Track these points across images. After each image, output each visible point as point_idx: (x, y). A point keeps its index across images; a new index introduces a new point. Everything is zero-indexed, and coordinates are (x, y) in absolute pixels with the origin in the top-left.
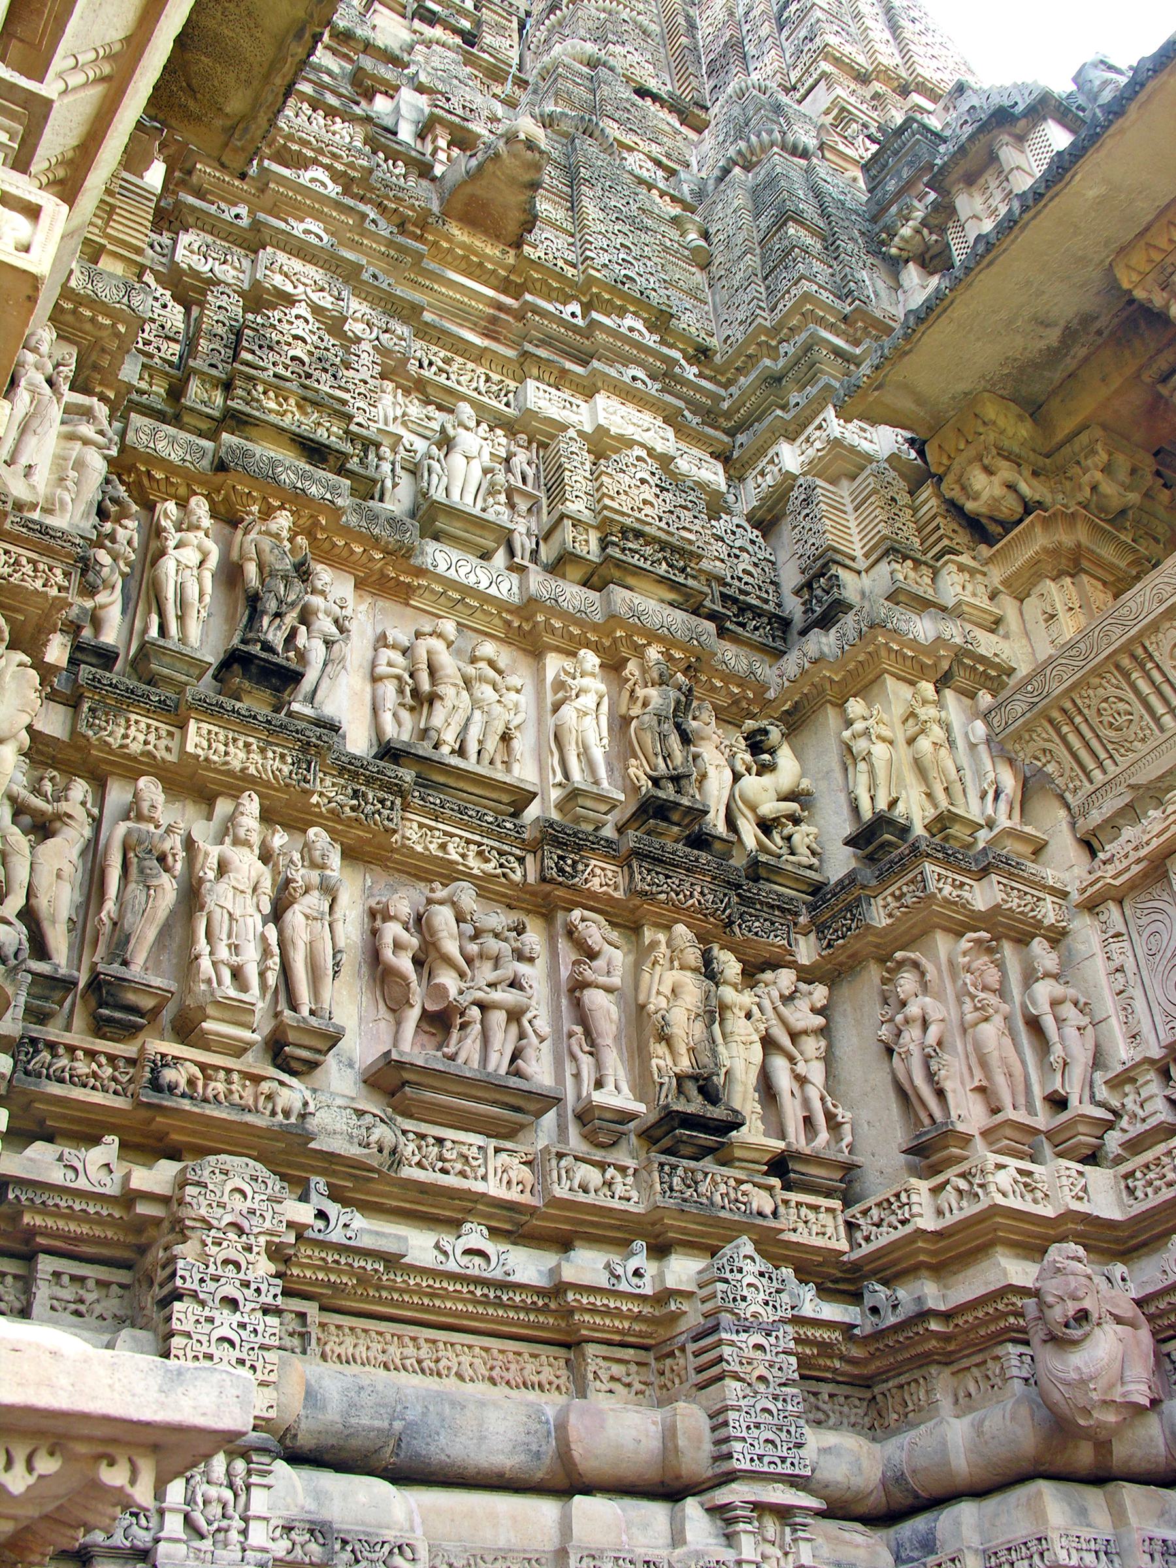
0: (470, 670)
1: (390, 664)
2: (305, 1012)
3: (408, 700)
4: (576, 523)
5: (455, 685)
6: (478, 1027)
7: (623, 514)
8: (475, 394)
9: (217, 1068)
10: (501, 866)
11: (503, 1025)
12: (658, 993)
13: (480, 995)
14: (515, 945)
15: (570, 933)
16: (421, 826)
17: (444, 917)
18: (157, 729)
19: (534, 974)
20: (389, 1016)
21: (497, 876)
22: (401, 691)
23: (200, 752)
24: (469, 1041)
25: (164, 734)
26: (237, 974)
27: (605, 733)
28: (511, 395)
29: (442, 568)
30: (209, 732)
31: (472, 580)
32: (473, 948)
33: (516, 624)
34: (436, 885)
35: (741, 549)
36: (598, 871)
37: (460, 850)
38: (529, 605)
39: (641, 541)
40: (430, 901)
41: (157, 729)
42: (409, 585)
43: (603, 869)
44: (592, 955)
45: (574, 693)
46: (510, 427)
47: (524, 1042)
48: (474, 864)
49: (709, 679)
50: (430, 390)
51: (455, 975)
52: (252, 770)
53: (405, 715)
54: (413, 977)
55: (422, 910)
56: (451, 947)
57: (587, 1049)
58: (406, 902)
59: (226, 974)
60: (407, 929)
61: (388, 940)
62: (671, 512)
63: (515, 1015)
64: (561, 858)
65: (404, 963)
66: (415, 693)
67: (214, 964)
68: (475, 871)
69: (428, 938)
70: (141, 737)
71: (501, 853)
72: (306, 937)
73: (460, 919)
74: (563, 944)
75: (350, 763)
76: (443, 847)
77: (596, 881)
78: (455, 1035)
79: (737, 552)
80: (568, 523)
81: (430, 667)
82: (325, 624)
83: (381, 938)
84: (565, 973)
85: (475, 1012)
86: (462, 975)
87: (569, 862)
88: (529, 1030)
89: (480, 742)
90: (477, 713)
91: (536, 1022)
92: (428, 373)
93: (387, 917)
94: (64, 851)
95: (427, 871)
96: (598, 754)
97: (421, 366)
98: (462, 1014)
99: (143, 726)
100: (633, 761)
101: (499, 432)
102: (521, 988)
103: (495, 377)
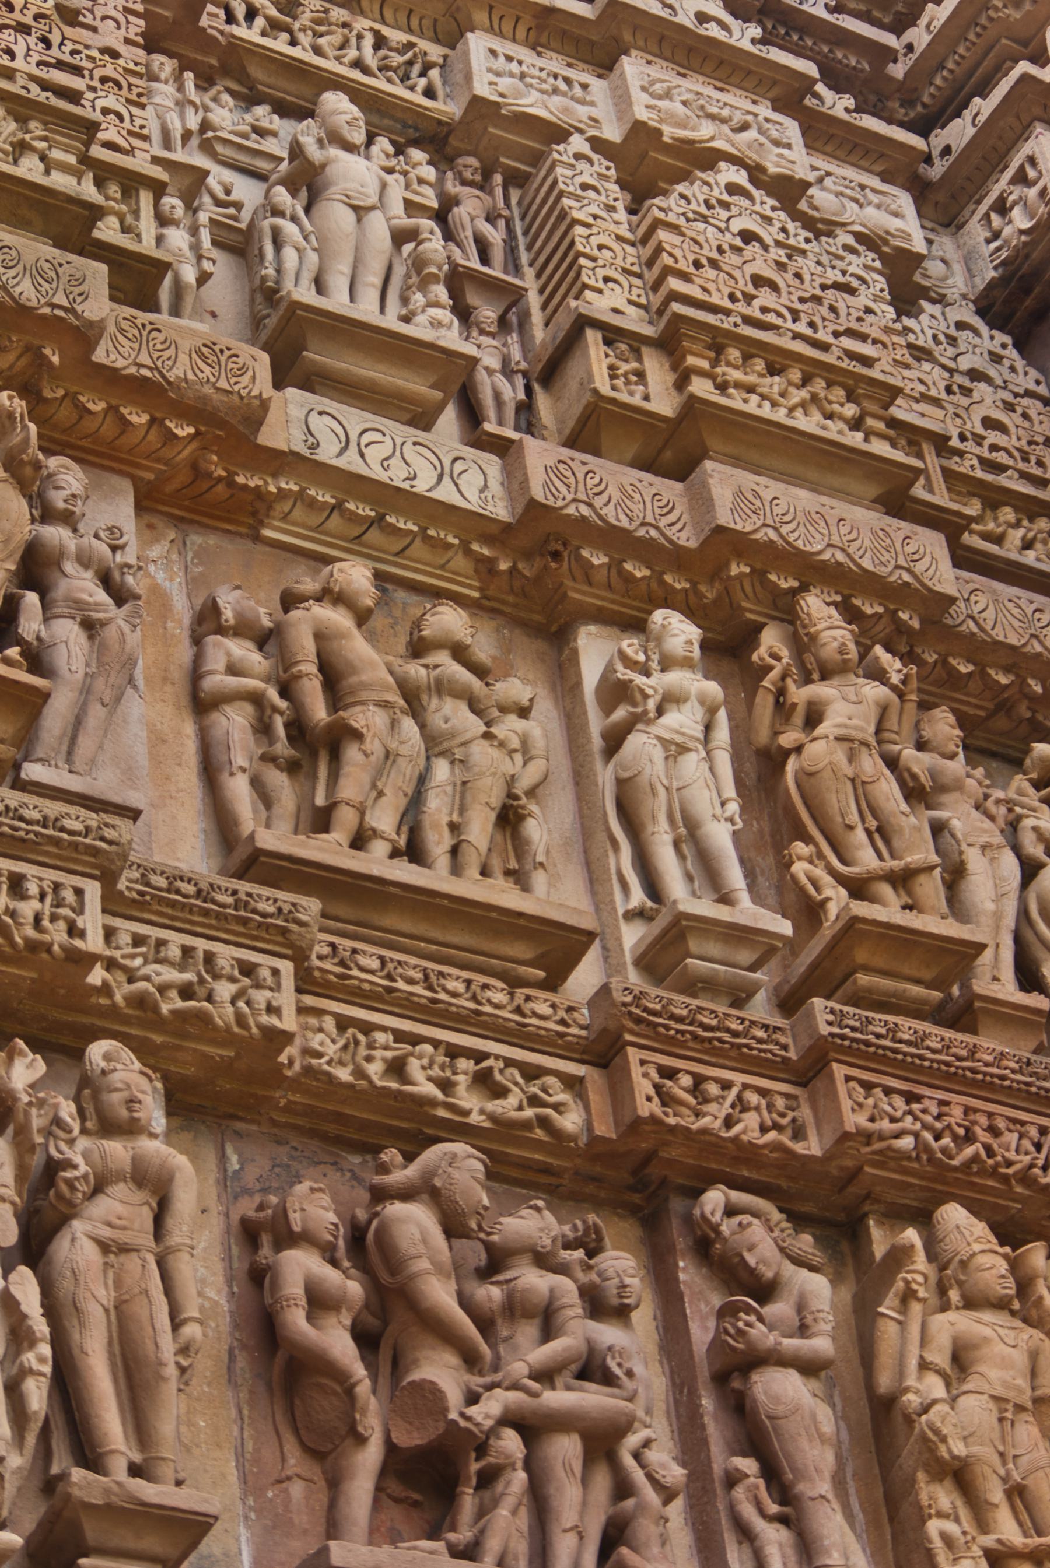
0: (416, 671)
2: (119, 1468)
3: (282, 747)
4: (612, 335)
5: (385, 705)
6: (520, 1477)
7: (714, 309)
8: (356, 75)
10: (534, 1101)
11: (578, 1467)
12: (924, 1366)
14: (583, 1277)
15: (706, 1245)
16: (343, 1023)
17: (414, 1223)
19: (633, 1342)
20: (314, 1470)
21: (526, 1125)
22: (263, 729)
24: (503, 1512)
27: (730, 791)
28: (434, 73)
29: (328, 453)
31: (396, 475)
33: (504, 566)
34: (391, 1155)
35: (975, 375)
36: (753, 1098)
37: (436, 1072)
39: (760, 365)
40: (380, 1195)
42: (258, 493)
43: (763, 1092)
44: (765, 1291)
45: (651, 704)
46: (437, 140)
47: (630, 1503)
48: (472, 1103)
49: (943, 661)
50: (256, 72)
51: (451, 1358)
53: (278, 780)
54: (360, 1371)
55: (362, 1215)
56: (441, 1294)
57: (774, 1508)
58: (326, 1199)
60: (334, 1263)
61: (294, 1288)
62: (817, 300)
63: (602, 1442)
65: (338, 1342)
66: (298, 729)
68: (475, 1118)
69: (385, 1277)
71: (531, 1073)
73: (453, 1227)
74: (688, 1272)
76: (397, 1068)
77: (751, 1120)
78: (468, 1501)
79: (966, 382)
80: (593, 337)
82: (81, 584)
83: (275, 1286)
84: (701, 1333)
85: (511, 1442)
86: (471, 1360)
87: (686, 1080)
88: (638, 1476)
89: (454, 827)
91: (654, 1456)
92: (250, 34)
93: (287, 1238)
95: (365, 1126)
96: (720, 836)
97: (231, 19)
98: (482, 1450)
100: (800, 848)
101: (417, 155)
102: (608, 1379)
103: (396, 36)
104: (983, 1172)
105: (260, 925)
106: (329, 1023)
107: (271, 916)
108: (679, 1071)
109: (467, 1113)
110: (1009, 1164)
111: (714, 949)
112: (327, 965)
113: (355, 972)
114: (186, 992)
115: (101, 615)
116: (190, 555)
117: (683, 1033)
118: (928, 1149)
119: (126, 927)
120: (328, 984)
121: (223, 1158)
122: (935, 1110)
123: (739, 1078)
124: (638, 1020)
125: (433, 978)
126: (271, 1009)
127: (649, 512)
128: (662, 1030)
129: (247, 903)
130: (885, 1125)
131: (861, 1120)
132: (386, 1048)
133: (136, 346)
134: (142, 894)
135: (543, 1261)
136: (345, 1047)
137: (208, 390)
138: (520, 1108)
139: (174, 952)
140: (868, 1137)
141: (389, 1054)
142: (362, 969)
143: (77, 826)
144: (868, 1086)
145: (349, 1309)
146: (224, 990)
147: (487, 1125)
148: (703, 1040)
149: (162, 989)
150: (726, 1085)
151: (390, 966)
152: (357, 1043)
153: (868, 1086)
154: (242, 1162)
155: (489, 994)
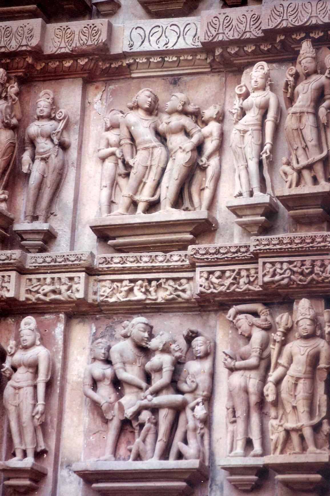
0: (162, 127)
1: (109, 145)
5: (146, 148)
13: (145, 402)
16: (113, 281)
21: (173, 299)
22: (117, 164)
32: (148, 365)
38: (208, 48)
68: (159, 300)
75: (44, 261)
85: (145, 415)
104: (318, 282)
105: (71, 265)
106: (108, 283)
107: (75, 260)
108: (214, 271)
109: (156, 300)
111: (248, 212)
112: (104, 266)
113: (114, 265)
114: (54, 292)
115: (48, 154)
116: (109, 94)
117: (214, 259)
118: (294, 281)
120: (105, 271)
121: (91, 329)
122: (299, 264)
123: (237, 267)
124: (198, 259)
125: (139, 258)
127: (248, 26)
128: (206, 260)
129: (68, 259)
130: (277, 278)
131: (267, 279)
132: (126, 286)
133: (60, 40)
134: (35, 267)
135: (166, 350)
136: (114, 289)
137: (84, 47)
138: (171, 294)
139: (48, 281)
140: (273, 282)
141: (126, 288)
142: (115, 263)
143: (3, 257)
144: (273, 264)
145: (108, 379)
146: (64, 288)
147: (163, 301)
148: (222, 258)
149: (45, 295)
150: (234, 271)
151: (124, 259)
152: (117, 286)
153: (273, 264)
154: (96, 329)
155: (158, 258)
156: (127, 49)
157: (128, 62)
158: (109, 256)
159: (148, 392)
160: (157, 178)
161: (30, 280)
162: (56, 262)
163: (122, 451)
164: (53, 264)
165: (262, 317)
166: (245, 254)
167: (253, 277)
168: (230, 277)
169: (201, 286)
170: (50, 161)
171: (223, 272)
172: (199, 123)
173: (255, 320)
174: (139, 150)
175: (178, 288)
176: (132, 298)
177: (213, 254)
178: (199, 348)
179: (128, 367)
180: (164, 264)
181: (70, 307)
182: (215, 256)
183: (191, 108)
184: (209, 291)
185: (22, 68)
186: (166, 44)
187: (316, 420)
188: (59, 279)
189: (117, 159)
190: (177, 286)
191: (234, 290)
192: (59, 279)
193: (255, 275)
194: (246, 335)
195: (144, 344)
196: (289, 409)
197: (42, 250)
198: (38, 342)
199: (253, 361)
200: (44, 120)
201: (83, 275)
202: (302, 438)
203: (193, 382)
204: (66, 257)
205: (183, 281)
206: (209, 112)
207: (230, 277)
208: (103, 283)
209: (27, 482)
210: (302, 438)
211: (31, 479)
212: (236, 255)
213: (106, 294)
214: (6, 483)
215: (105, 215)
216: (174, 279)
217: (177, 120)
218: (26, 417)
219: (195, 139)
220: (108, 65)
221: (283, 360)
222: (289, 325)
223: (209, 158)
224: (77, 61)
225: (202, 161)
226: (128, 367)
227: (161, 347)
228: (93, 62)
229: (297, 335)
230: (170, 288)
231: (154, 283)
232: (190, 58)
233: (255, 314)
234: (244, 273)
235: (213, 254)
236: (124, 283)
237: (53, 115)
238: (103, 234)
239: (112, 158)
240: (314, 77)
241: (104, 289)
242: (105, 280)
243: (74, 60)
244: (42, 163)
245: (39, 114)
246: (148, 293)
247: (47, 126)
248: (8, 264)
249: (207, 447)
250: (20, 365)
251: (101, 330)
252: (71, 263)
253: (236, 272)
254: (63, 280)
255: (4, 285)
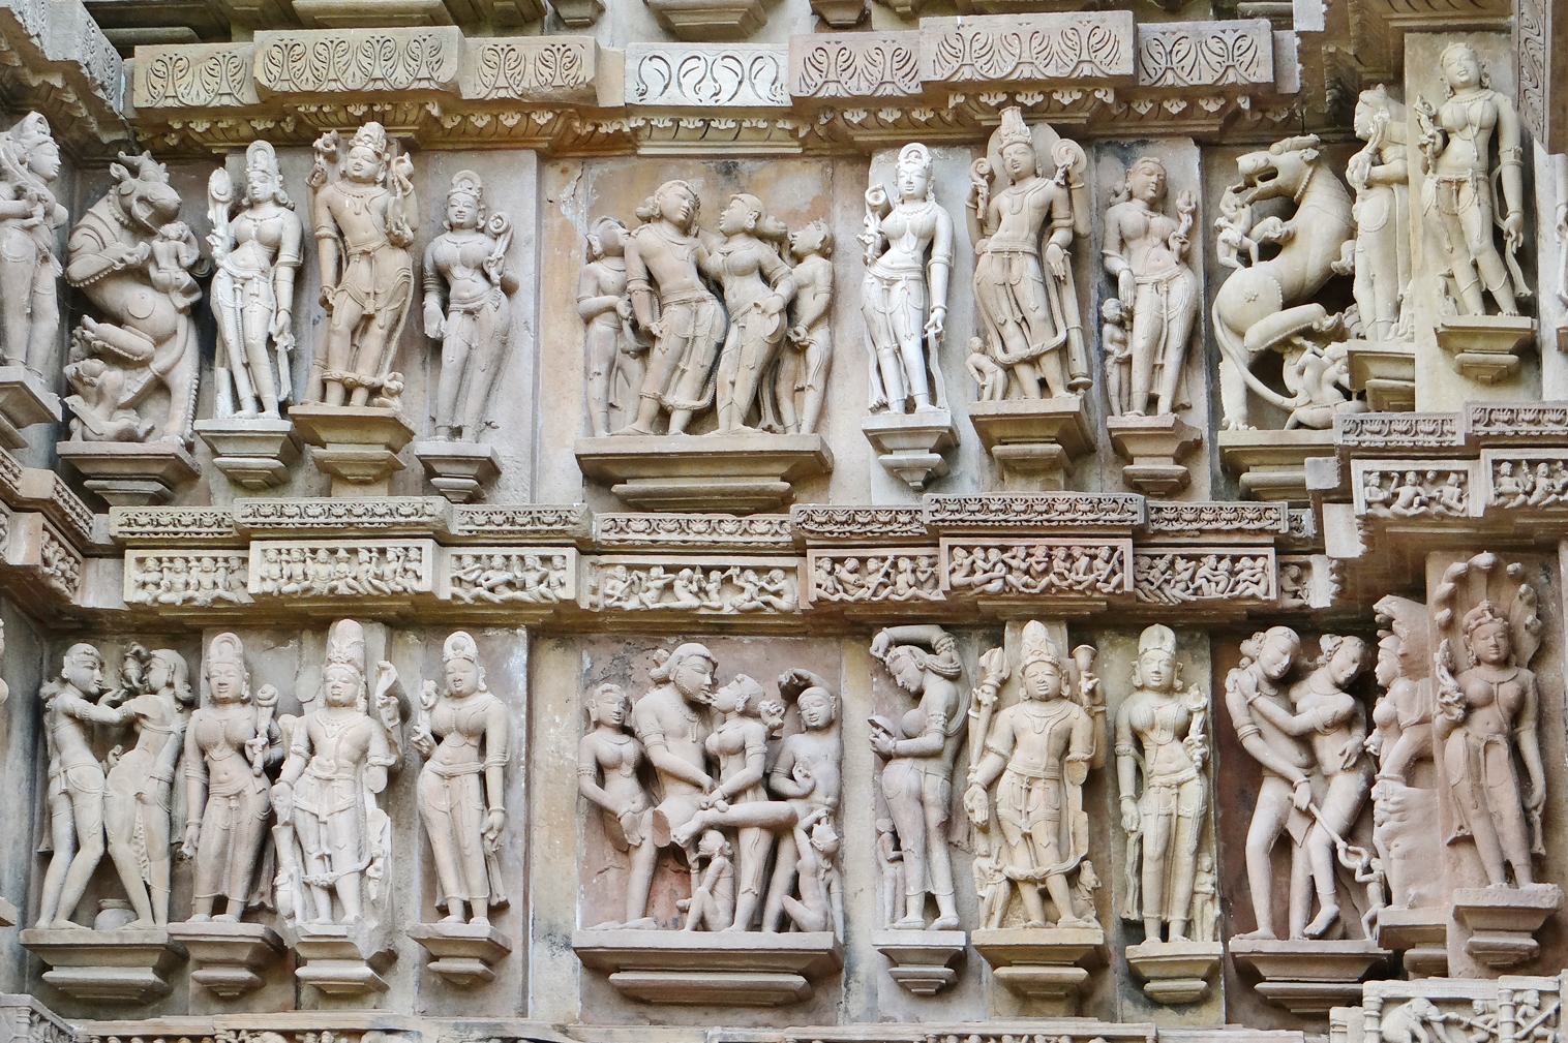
0: (714, 263)
1: (600, 290)
3: (630, 340)
5: (684, 302)
9: (304, 1032)
12: (985, 749)
13: (712, 815)
15: (882, 669)
16: (630, 568)
18: (226, 560)
21: (757, 609)
23: (269, 587)
25: (235, 564)
26: (332, 891)
30: (280, 551)
41: (226, 560)
43: (912, 558)
52: (343, 590)
59: (323, 899)
64: (835, 560)
67: (308, 885)
68: (727, 610)
70: (207, 581)
72: (444, 804)
75: (490, 522)
76: (669, 587)
81: (652, 280)
82: (466, 283)
90: (734, 329)
94: (141, 767)
99: (207, 563)
106: (620, 571)
109: (720, 609)
110: (1080, 583)
112: (613, 536)
113: (632, 536)
114: (510, 584)
119: (467, 553)
120: (614, 547)
123: (891, 553)
124: (812, 532)
125: (684, 525)
126: (562, 584)
135: (749, 713)
138: (752, 599)
139: (498, 561)
140: (969, 587)
141: (660, 583)
146: (531, 578)
147: (735, 613)
149: (492, 590)
150: (884, 559)
151: (654, 524)
155: (723, 525)
156: (634, 99)
157: (633, 125)
158: (622, 516)
159: (717, 794)
160: (708, 363)
161: (459, 558)
162: (513, 523)
163: (661, 908)
164: (507, 527)
165: (945, 654)
166: (908, 527)
167: (924, 572)
168: (878, 570)
169: (819, 586)
170: (482, 315)
171: (863, 561)
172: (786, 256)
173: (928, 659)
174: (669, 304)
175: (767, 586)
176: (668, 602)
177: (842, 523)
178: (814, 710)
179: (671, 743)
180: (737, 538)
181: (541, 616)
182: (848, 528)
183: (770, 225)
184: (836, 598)
185: (414, 123)
186: (716, 94)
187: (1072, 863)
188: (522, 558)
189: (620, 319)
190: (763, 584)
191: (886, 598)
192: (522, 558)
193: (930, 570)
194: (913, 689)
195: (702, 697)
196: (1015, 838)
197: (473, 498)
198: (483, 686)
199: (931, 740)
200: (467, 231)
201: (571, 552)
202: (1045, 896)
203: (806, 776)
204: (535, 515)
205: (777, 574)
206: (806, 237)
207: (878, 570)
208: (610, 571)
209: (477, 966)
210: (1045, 896)
211: (484, 961)
212: (889, 528)
213: (617, 594)
214: (433, 965)
215: (602, 434)
216: (758, 570)
217: (748, 251)
218: (471, 838)
219: (784, 290)
220: (590, 128)
221: (998, 742)
222: (1005, 675)
223: (811, 327)
224: (528, 115)
225: (798, 334)
226: (671, 743)
227: (740, 706)
228: (561, 120)
229: (1022, 693)
230: (748, 586)
231: (715, 575)
232: (763, 125)
233: (928, 647)
234: (904, 564)
235: (842, 523)
236: (654, 572)
237: (482, 223)
238: (599, 473)
239: (610, 315)
240: (1032, 182)
241: (611, 582)
242: (615, 565)
243: (522, 113)
244: (468, 320)
245: (455, 220)
246: (702, 595)
247: (476, 245)
248: (418, 524)
249: (837, 907)
250: (450, 731)
251: (600, 666)
252: (545, 527)
253: (888, 563)
254: (528, 561)
255: (408, 566)
